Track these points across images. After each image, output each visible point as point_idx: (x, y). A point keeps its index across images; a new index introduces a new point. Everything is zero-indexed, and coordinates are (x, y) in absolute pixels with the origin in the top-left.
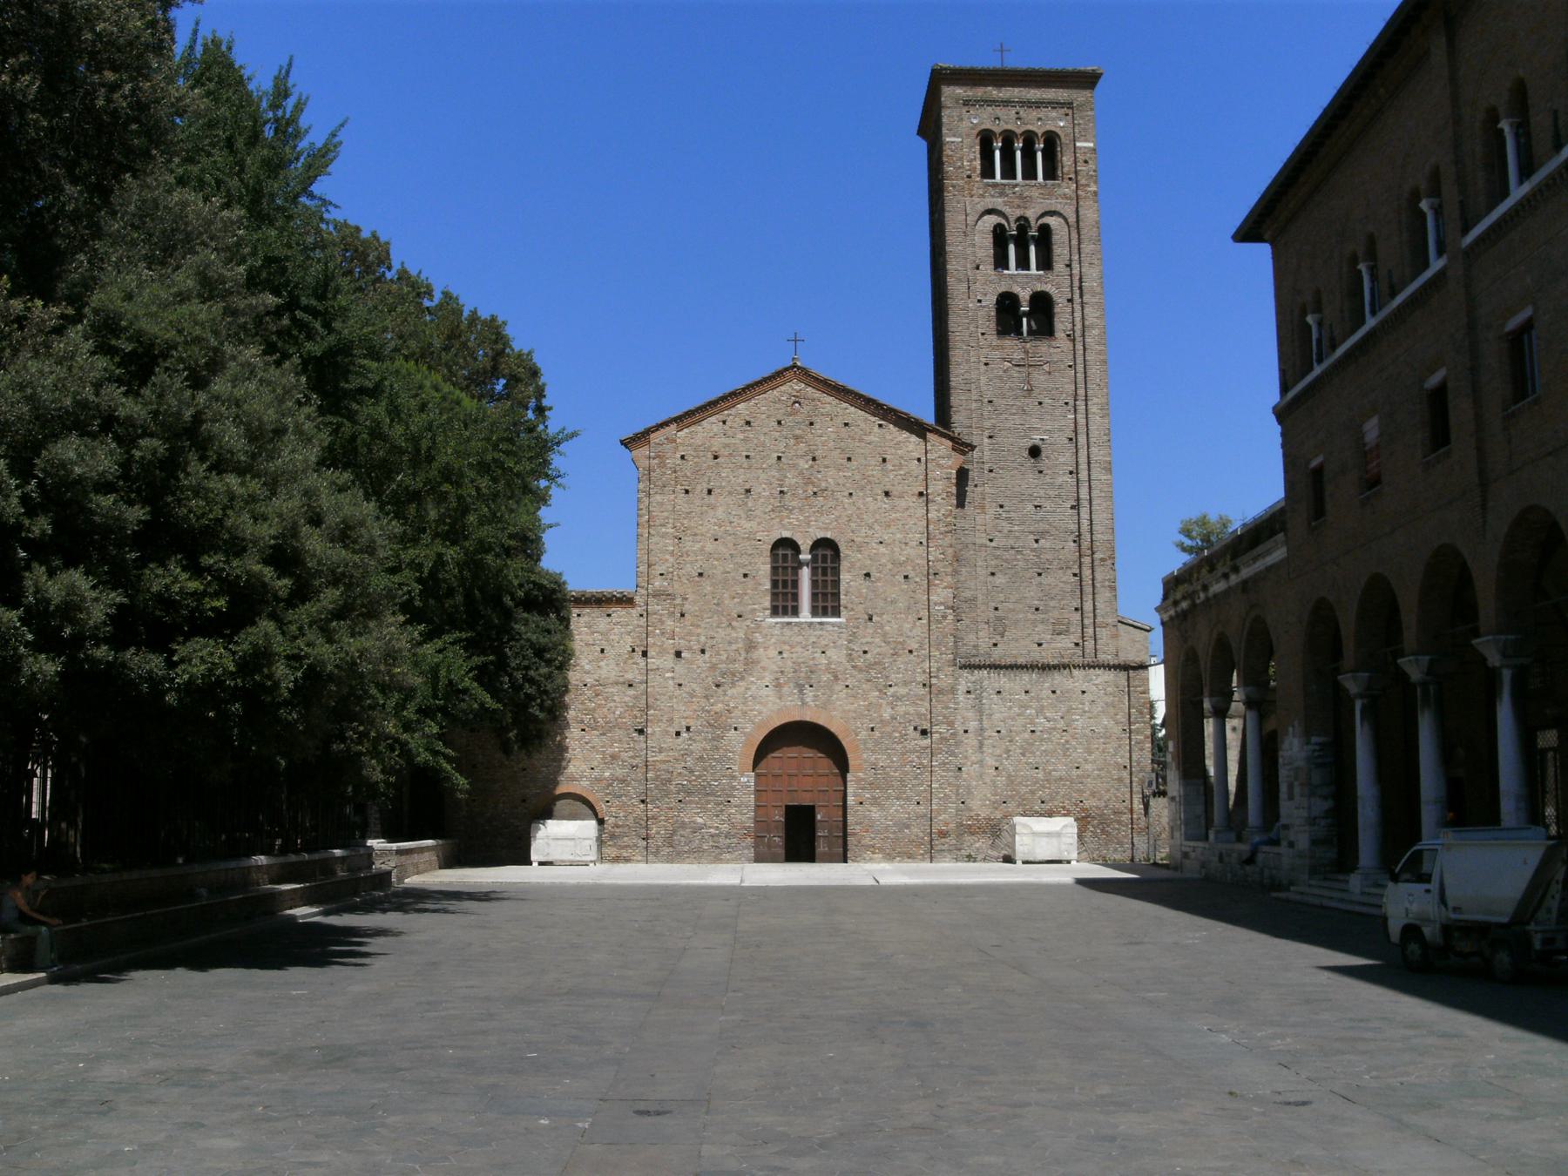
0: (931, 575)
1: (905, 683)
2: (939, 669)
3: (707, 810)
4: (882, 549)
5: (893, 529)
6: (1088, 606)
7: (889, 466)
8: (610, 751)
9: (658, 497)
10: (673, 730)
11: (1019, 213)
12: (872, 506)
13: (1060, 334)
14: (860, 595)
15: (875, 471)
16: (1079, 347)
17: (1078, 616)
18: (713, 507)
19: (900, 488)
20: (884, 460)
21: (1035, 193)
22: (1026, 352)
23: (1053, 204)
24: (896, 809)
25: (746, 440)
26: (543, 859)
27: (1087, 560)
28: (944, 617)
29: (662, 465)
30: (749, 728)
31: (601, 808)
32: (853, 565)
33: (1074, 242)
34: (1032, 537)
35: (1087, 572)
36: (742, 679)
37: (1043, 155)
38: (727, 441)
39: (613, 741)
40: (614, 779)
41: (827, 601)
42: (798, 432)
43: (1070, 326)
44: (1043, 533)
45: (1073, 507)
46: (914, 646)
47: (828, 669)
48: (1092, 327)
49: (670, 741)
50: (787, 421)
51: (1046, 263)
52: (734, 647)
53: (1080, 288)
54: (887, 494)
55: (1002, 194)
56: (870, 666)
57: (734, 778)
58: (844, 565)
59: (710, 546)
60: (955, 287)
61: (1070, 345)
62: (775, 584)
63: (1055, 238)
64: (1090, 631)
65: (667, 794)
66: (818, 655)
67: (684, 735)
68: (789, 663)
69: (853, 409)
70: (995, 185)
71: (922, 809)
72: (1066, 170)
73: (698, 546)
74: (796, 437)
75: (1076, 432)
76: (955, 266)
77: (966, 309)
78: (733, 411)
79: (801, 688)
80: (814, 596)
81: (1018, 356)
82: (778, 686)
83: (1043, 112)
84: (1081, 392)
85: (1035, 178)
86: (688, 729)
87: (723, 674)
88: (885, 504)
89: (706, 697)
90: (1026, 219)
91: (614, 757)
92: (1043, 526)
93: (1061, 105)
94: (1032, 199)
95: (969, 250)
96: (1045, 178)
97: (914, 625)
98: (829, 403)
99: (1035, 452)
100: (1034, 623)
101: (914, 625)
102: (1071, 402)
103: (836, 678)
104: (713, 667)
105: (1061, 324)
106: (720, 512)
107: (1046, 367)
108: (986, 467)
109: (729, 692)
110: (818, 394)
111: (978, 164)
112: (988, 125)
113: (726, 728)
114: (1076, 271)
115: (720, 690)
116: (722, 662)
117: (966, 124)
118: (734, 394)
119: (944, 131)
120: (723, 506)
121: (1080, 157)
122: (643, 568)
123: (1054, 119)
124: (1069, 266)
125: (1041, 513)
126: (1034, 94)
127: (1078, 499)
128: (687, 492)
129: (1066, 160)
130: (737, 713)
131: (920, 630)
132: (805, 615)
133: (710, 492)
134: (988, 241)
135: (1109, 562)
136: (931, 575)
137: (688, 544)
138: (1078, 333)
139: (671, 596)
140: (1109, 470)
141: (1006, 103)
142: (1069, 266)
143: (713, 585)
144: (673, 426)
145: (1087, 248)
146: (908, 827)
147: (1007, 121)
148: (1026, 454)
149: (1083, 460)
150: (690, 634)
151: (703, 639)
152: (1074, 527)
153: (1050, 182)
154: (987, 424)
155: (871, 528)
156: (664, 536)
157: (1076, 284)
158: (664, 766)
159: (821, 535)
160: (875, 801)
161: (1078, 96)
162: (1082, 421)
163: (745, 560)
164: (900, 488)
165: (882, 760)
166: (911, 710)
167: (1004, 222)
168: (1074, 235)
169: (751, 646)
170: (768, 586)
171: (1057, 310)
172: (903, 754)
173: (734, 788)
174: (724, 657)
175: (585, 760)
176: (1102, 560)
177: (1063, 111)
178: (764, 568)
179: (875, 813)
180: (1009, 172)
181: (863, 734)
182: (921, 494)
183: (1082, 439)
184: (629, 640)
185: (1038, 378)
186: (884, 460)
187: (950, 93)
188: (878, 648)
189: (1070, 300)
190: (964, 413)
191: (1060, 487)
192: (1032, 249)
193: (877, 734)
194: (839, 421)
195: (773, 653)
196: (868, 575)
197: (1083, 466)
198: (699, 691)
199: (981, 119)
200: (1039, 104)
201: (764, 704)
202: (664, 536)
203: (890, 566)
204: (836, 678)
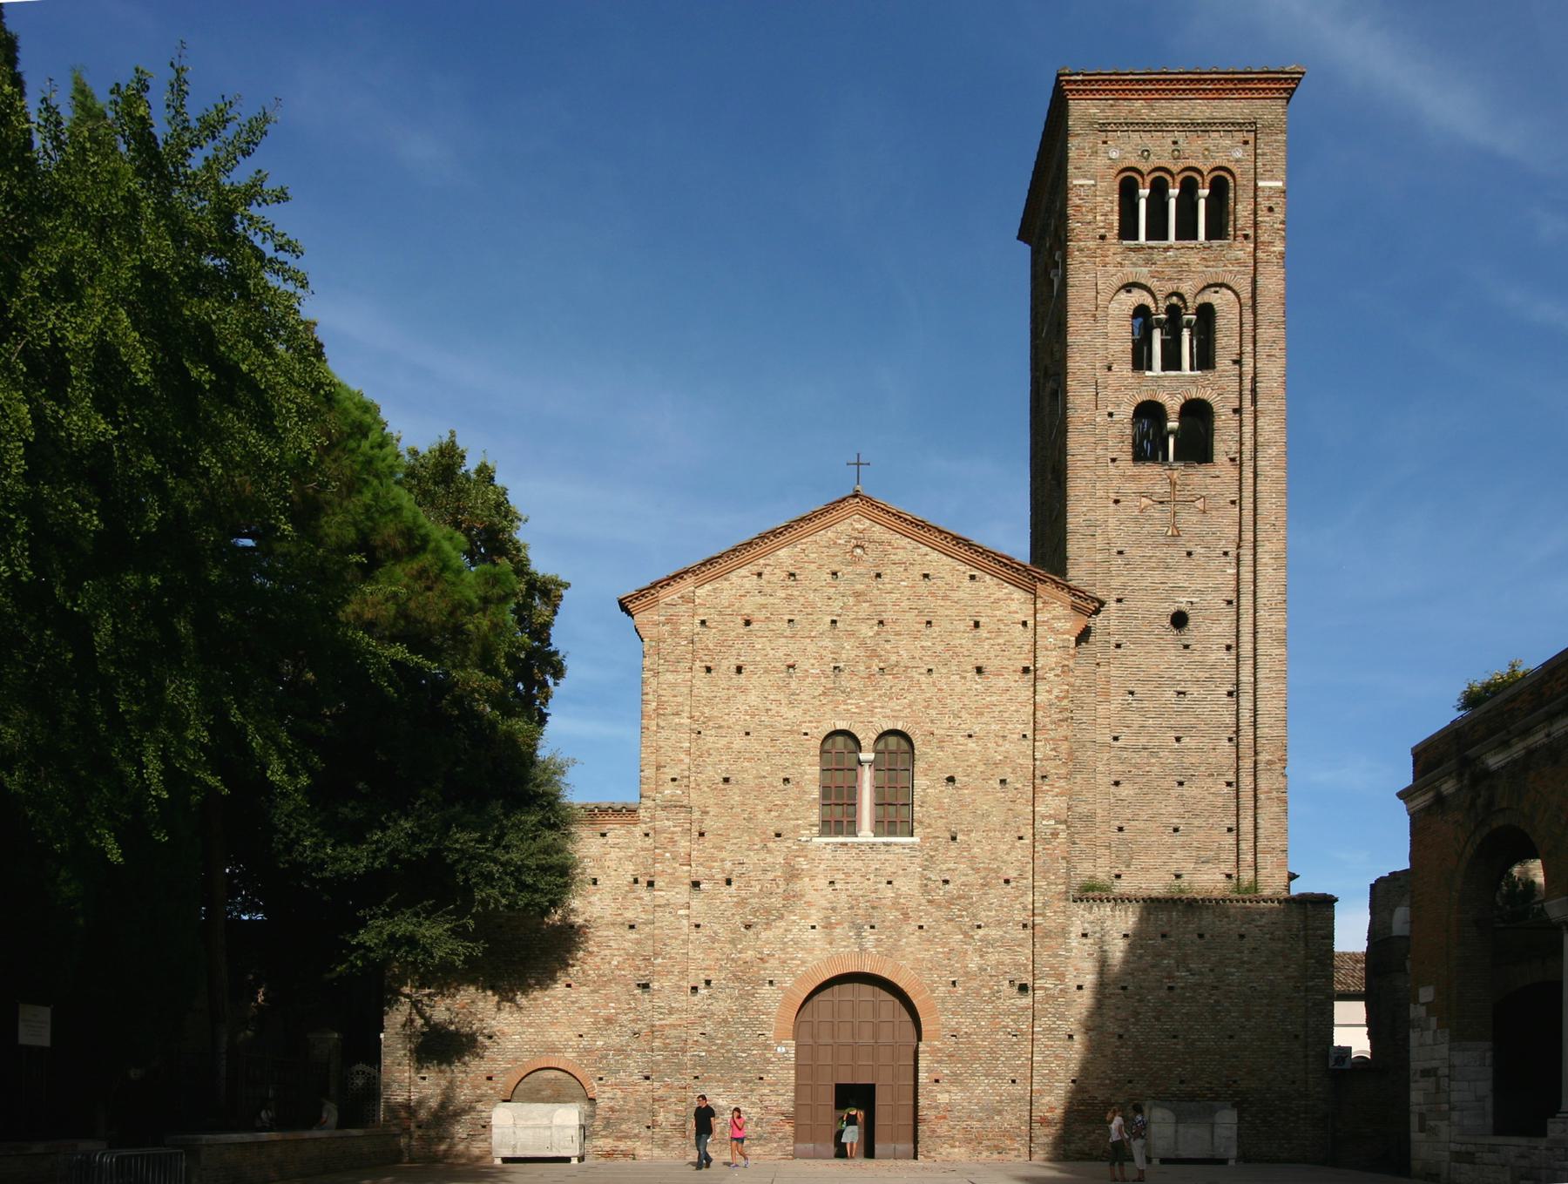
0: (1038, 778)
1: (999, 923)
3: (730, 1089)
4: (971, 744)
5: (984, 720)
6: (1247, 825)
8: (603, 1013)
9: (670, 677)
10: (686, 985)
11: (1170, 287)
13: (1220, 456)
14: (940, 807)
15: (964, 640)
18: (744, 691)
19: (997, 662)
20: (977, 625)
21: (1194, 259)
23: (1218, 273)
24: (983, 1089)
25: (789, 598)
26: (508, 1154)
27: (1247, 764)
29: (675, 633)
30: (789, 982)
31: (595, 1089)
32: (931, 767)
33: (1248, 327)
35: (1246, 781)
36: (781, 917)
37: (1207, 207)
38: (761, 600)
39: (608, 999)
40: (607, 1048)
41: (895, 815)
42: (859, 587)
43: (1235, 447)
47: (895, 904)
48: (1268, 444)
49: (683, 1000)
50: (844, 570)
52: (770, 876)
53: (1254, 391)
54: (979, 670)
55: (1149, 262)
56: (951, 902)
57: (767, 1047)
58: (920, 765)
59: (739, 743)
60: (1079, 396)
62: (825, 790)
63: (1220, 323)
64: (1248, 858)
65: (680, 1067)
66: (883, 885)
67: (703, 991)
68: (843, 896)
70: (1140, 249)
71: (1017, 1090)
72: (1240, 223)
73: (723, 742)
74: (857, 595)
76: (1079, 366)
77: (1093, 423)
78: (771, 560)
79: (859, 929)
80: (879, 804)
82: (829, 926)
83: (1216, 139)
84: (1248, 536)
85: (1195, 237)
86: (708, 982)
87: (754, 912)
88: (977, 684)
89: (733, 942)
90: (1181, 296)
91: (609, 1021)
93: (1239, 125)
94: (1187, 268)
95: (1099, 342)
96: (1208, 237)
97: (1013, 847)
98: (904, 547)
101: (1013, 847)
103: (905, 915)
104: (742, 902)
105: (1223, 445)
106: (753, 698)
109: (763, 935)
110: (888, 536)
111: (1115, 217)
112: (1133, 161)
113: (758, 983)
114: (1248, 368)
115: (750, 933)
116: (755, 895)
117: (1101, 161)
118: (775, 533)
119: (1071, 170)
120: (756, 692)
121: (1264, 204)
122: (649, 772)
124: (1238, 362)
126: (1200, 109)
128: (709, 670)
129: (1242, 211)
130: (773, 963)
131: (1021, 852)
132: (866, 834)
133: (739, 670)
135: (1278, 766)
136: (1038, 778)
137: (710, 738)
138: (1247, 455)
139: (689, 809)
140: (1283, 642)
141: (1160, 126)
142: (1238, 362)
143: (744, 794)
144: (690, 579)
145: (1265, 333)
146: (999, 1113)
147: (1160, 152)
149: (1246, 629)
150: (713, 859)
151: (728, 865)
153: (1215, 243)
156: (677, 728)
158: (674, 1032)
159: (888, 725)
160: (955, 1079)
161: (1268, 110)
162: (1247, 575)
163: (786, 760)
164: (997, 662)
165: (966, 1025)
166: (1007, 959)
168: (1248, 317)
169: (792, 875)
170: (816, 793)
171: (1218, 424)
172: (994, 1017)
173: (768, 1061)
174: (757, 890)
175: (571, 1025)
176: (1270, 762)
177: (1239, 136)
178: (811, 771)
179: (957, 1095)
180: (1157, 230)
181: (942, 991)
183: (1246, 601)
184: (630, 867)
187: (1081, 110)
188: (963, 874)
189: (1238, 411)
190: (1086, 566)
192: (1186, 334)
193: (960, 990)
194: (917, 572)
195: (822, 882)
196: (951, 779)
197: (1246, 638)
198: (723, 934)
199: (1122, 151)
200: (1205, 127)
201: (810, 951)
202: (677, 728)
203: (981, 767)
204: (905, 915)
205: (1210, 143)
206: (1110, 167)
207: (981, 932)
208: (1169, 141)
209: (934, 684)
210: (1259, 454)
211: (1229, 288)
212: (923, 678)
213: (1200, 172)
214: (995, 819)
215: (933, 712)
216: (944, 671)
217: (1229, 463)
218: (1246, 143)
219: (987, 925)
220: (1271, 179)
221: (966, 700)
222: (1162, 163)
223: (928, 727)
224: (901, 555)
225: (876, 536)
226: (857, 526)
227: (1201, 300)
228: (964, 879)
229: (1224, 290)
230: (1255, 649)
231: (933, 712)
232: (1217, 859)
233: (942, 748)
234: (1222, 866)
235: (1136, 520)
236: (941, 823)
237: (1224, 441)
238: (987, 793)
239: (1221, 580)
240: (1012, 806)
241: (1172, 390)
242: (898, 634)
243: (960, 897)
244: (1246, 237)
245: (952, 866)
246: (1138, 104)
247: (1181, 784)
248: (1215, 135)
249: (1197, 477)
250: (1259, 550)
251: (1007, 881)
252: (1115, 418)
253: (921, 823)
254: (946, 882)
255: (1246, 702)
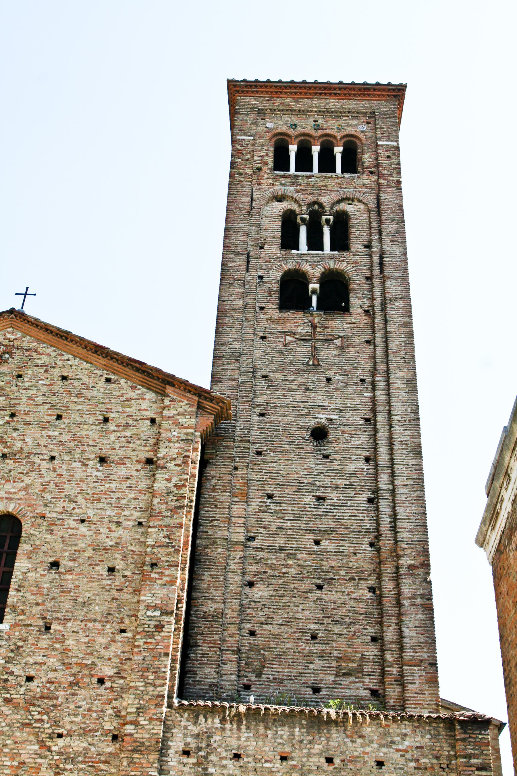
1: (85, 732)
2: (140, 710)
4: (83, 529)
5: (99, 505)
6: (390, 634)
7: (111, 426)
12: (79, 474)
16: (379, 320)
17: (372, 651)
22: (314, 327)
23: (349, 191)
27: (388, 569)
28: (159, 627)
34: (311, 536)
35: (388, 586)
44: (326, 533)
45: (370, 501)
46: (108, 671)
51: (341, 243)
54: (102, 460)
58: (24, 548)
61: (366, 320)
69: (76, 361)
72: (366, 164)
75: (374, 411)
81: (304, 330)
84: (381, 366)
92: (325, 524)
96: (343, 172)
99: (319, 434)
100: (309, 657)
102: (368, 380)
107: (338, 342)
108: (254, 448)
123: (354, 126)
124: (368, 246)
125: (326, 506)
127: (376, 491)
129: (367, 158)
134: (277, 225)
148: (307, 435)
152: (369, 525)
153: (347, 175)
154: (259, 400)
155: (72, 501)
157: (376, 259)
167: (295, 207)
168: (374, 218)
177: (363, 119)
182: (149, 461)
185: (328, 353)
186: (106, 420)
191: (353, 475)
196: (55, 565)
197: (383, 450)
203: (89, 553)
205: (341, 122)
206: (266, 132)
207: (61, 742)
208: (312, 120)
209: (54, 470)
210: (388, 306)
211: (360, 201)
212: (44, 464)
213: (335, 137)
214: (98, 609)
215: (48, 496)
216: (66, 458)
217: (363, 314)
218: (368, 123)
219: (69, 735)
220: (388, 140)
221: (84, 486)
222: (306, 131)
223: (40, 510)
224: (45, 359)
225: (25, 345)
226: (9, 336)
227: (336, 208)
228: (51, 675)
229: (356, 202)
230: (392, 460)
231: (48, 496)
232: (359, 672)
233: (51, 532)
234: (367, 680)
235: (280, 352)
236: (36, 610)
237: (359, 298)
238: (91, 580)
239: (358, 401)
240: (116, 594)
241: (314, 263)
242: (28, 424)
243: (42, 697)
244: (371, 173)
245: (40, 659)
246: (288, 100)
247: (320, 587)
248: (347, 118)
249: (336, 323)
250: (392, 376)
251: (101, 681)
252: (265, 279)
253: (14, 609)
254: (29, 679)
255: (384, 507)
